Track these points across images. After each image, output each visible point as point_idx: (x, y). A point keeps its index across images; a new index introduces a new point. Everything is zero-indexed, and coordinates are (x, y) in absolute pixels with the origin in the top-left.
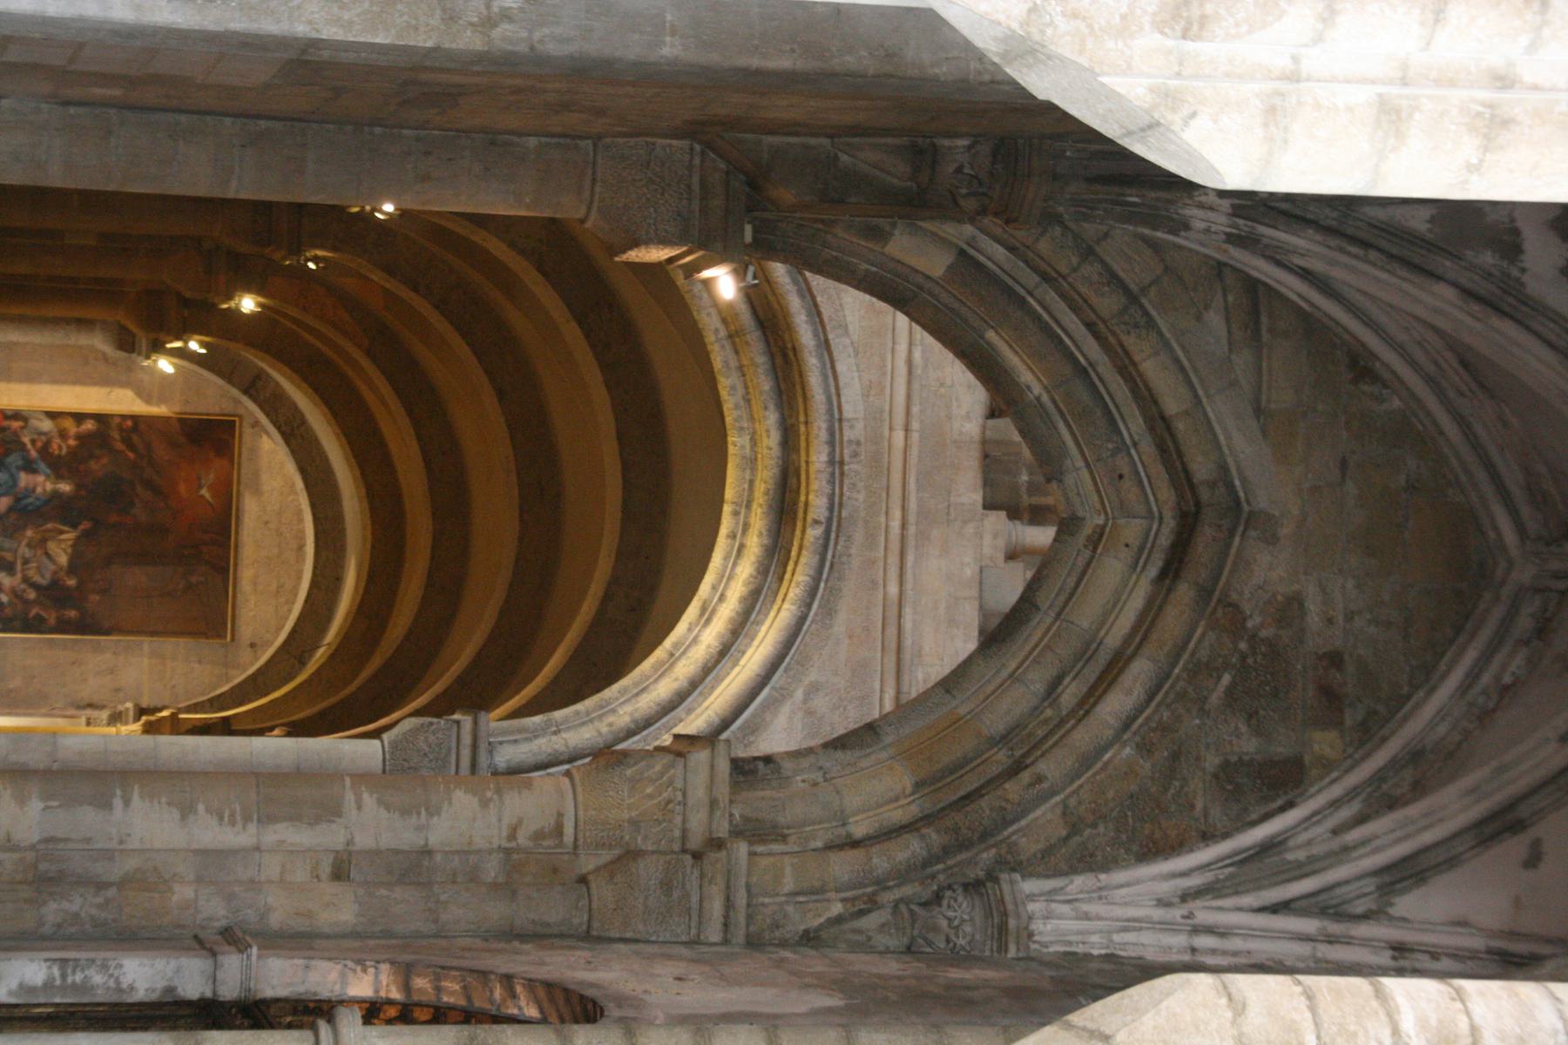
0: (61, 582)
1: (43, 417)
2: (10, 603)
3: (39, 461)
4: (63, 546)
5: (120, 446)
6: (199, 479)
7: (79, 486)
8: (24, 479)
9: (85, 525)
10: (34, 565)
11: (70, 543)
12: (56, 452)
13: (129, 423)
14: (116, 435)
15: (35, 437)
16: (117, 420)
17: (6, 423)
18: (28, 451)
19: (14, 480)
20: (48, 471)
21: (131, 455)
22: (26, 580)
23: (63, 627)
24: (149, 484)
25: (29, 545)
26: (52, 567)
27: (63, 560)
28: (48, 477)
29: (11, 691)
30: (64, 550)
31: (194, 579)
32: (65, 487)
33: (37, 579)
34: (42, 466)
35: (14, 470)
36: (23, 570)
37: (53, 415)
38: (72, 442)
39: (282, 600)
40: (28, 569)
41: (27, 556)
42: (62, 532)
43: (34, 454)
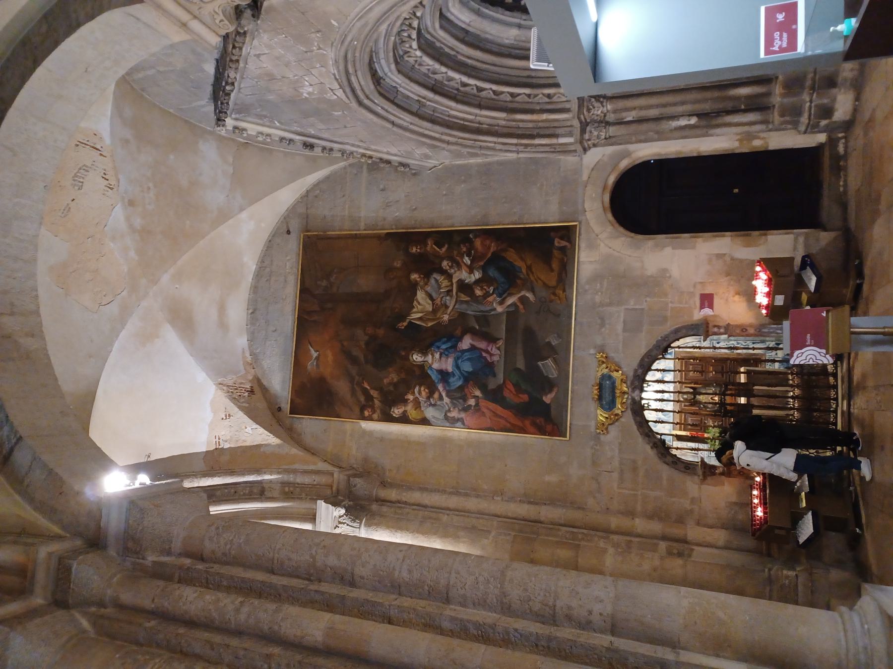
0: (422, 276)
1: (432, 420)
2: (462, 257)
3: (436, 381)
5: (374, 393)
6: (317, 364)
8: (448, 365)
11: (414, 310)
12: (422, 389)
13: (366, 413)
14: (376, 402)
15: (439, 403)
16: (375, 416)
17: (462, 415)
18: (445, 388)
19: (458, 367)
20: (429, 372)
21: (366, 386)
22: (450, 277)
23: (420, 237)
25: (447, 307)
26: (428, 289)
27: (420, 295)
29: (464, 181)
30: (419, 303)
31: (324, 283)
32: (417, 358)
33: (441, 278)
34: (434, 376)
35: (457, 372)
36: (452, 285)
37: (424, 422)
38: (411, 397)
39: (268, 270)
40: (447, 287)
41: (448, 298)
42: (420, 319)
43: (440, 387)
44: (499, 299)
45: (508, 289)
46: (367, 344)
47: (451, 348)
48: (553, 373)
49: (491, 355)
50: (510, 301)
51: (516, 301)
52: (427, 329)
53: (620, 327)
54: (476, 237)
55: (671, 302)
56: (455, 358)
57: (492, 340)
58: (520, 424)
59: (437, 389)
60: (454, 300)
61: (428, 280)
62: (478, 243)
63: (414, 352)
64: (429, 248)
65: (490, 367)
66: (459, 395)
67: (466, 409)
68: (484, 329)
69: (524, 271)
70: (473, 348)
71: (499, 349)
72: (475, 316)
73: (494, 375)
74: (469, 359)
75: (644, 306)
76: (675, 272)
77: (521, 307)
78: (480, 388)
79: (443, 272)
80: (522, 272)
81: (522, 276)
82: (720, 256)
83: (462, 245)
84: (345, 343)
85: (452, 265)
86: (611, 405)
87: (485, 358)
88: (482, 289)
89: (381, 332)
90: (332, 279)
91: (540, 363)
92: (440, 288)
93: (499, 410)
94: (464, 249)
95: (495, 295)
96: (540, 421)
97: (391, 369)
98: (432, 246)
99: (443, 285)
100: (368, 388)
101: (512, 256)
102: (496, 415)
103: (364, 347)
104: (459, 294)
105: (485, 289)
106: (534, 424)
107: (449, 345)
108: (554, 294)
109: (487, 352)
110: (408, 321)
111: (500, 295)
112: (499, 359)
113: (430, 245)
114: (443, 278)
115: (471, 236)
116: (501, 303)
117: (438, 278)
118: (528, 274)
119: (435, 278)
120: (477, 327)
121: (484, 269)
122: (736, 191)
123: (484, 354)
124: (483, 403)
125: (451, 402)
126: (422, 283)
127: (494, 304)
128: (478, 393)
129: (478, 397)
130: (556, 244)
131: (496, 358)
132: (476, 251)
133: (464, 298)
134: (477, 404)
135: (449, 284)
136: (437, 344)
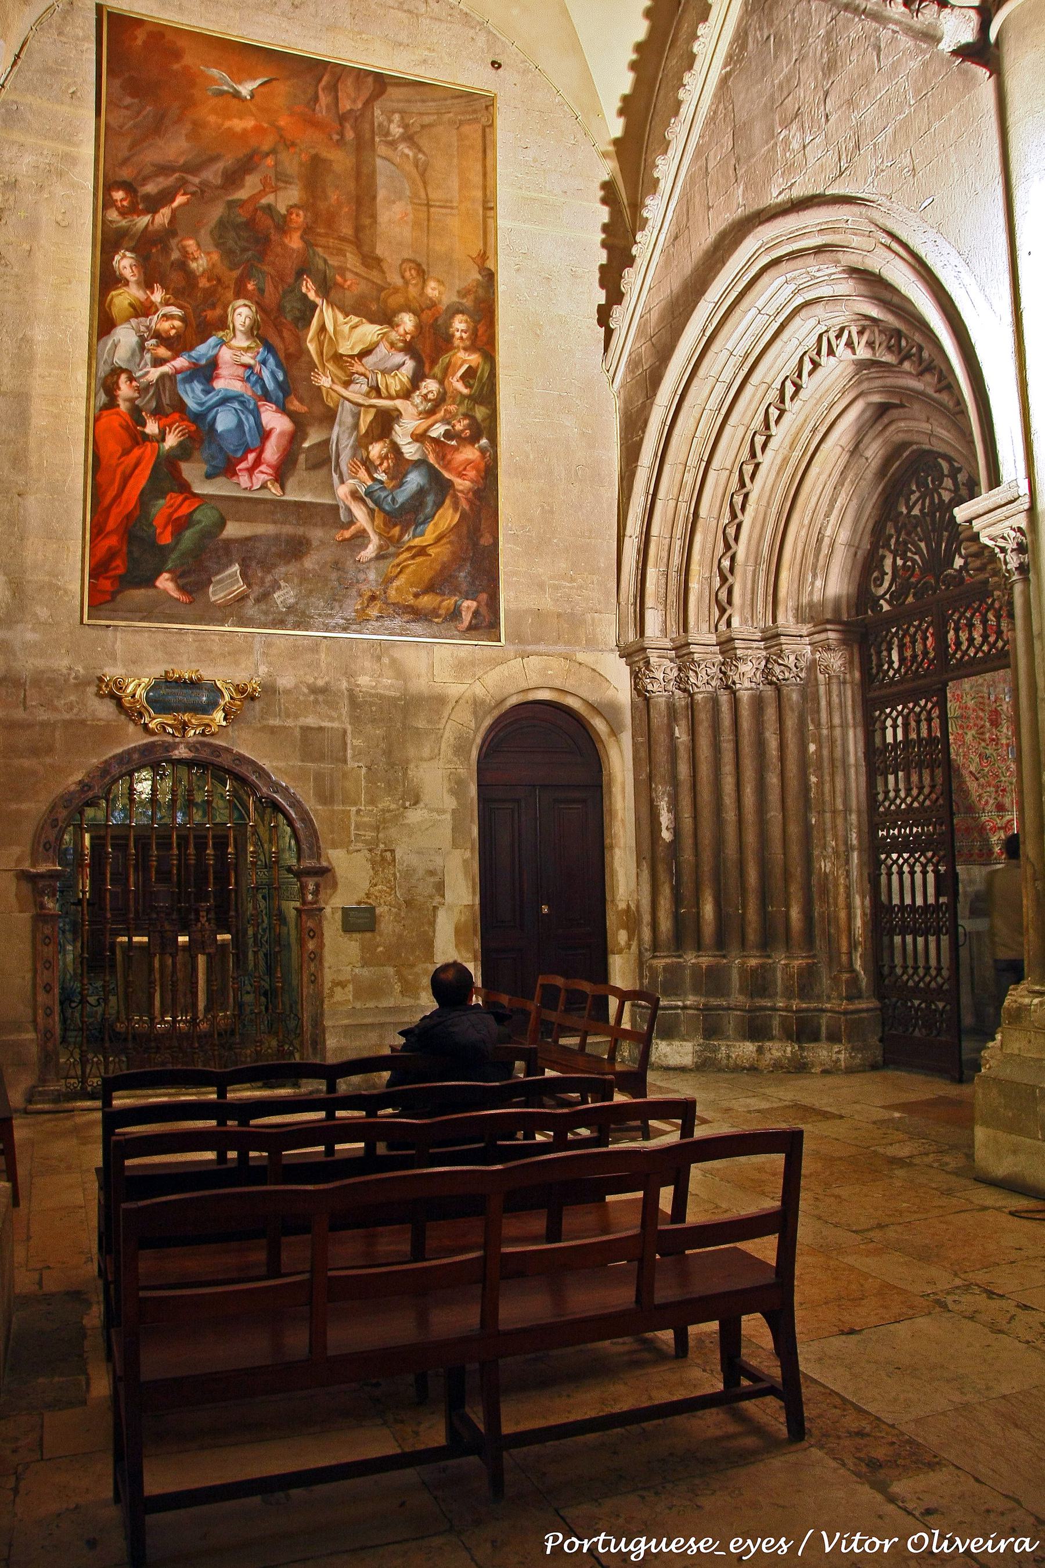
0: (408, 338)
2: (446, 421)
3: (193, 354)
4: (346, 328)
5: (163, 216)
6: (222, 93)
7: (240, 292)
8: (227, 383)
9: (309, 289)
10: (379, 376)
11: (340, 317)
12: (177, 323)
13: (119, 195)
14: (144, 220)
15: (148, 356)
17: (123, 406)
18: (178, 372)
19: (225, 400)
20: (212, 341)
21: (180, 200)
24: (233, 178)
25: (347, 384)
26: (383, 349)
27: (370, 331)
28: (222, 343)
31: (396, 130)
32: (242, 314)
34: (203, 350)
36: (390, 397)
38: (157, 296)
41: (365, 388)
42: (323, 328)
43: (181, 362)
44: (362, 491)
45: (381, 509)
46: (269, 209)
47: (264, 387)
48: (216, 594)
49: (251, 471)
50: (360, 513)
51: (358, 524)
52: (300, 341)
53: (311, 721)
54: (483, 451)
55: (358, 811)
56: (242, 396)
57: (281, 474)
58: (111, 524)
59: (176, 355)
60: (361, 401)
61: (401, 350)
62: (470, 453)
63: (254, 309)
64: (462, 355)
65: (228, 469)
66: (166, 400)
67: (137, 415)
68: (302, 457)
69: (417, 542)
70: (265, 435)
71: (263, 486)
72: (327, 442)
73: (209, 476)
74: (240, 424)
75: (351, 764)
76: (415, 816)
77: (347, 534)
78: (180, 444)
79: (416, 380)
80: (414, 537)
81: (406, 538)
82: (440, 888)
83: (466, 422)
84: (270, 161)
85: (430, 400)
86: (160, 705)
87: (244, 458)
88: (384, 458)
89: (295, 242)
90: (403, 148)
91: (236, 568)
92: (384, 372)
93: (140, 481)
94: (459, 427)
95: (370, 483)
96: (119, 566)
97: (215, 257)
98: (464, 361)
99: (390, 380)
100: (175, 204)
101: (447, 518)
102: (126, 479)
103: (264, 201)
104: (373, 411)
105: (381, 464)
106: (112, 555)
107: (270, 385)
108: (373, 598)
109: (258, 462)
110: (318, 301)
111: (369, 494)
112: (244, 486)
113: (467, 359)
114: (405, 380)
115: (484, 441)
116: (355, 495)
117: (403, 370)
118: (410, 548)
119: (404, 364)
120: (306, 445)
121: (421, 463)
122: (545, 909)
123: (251, 457)
124: (147, 454)
125: (148, 386)
126: (394, 336)
127: (351, 481)
128: (171, 441)
129: (163, 440)
130: (467, 603)
131: (244, 480)
132: (456, 449)
133: (366, 420)
134: (146, 437)
135: (393, 393)
136: (271, 361)
